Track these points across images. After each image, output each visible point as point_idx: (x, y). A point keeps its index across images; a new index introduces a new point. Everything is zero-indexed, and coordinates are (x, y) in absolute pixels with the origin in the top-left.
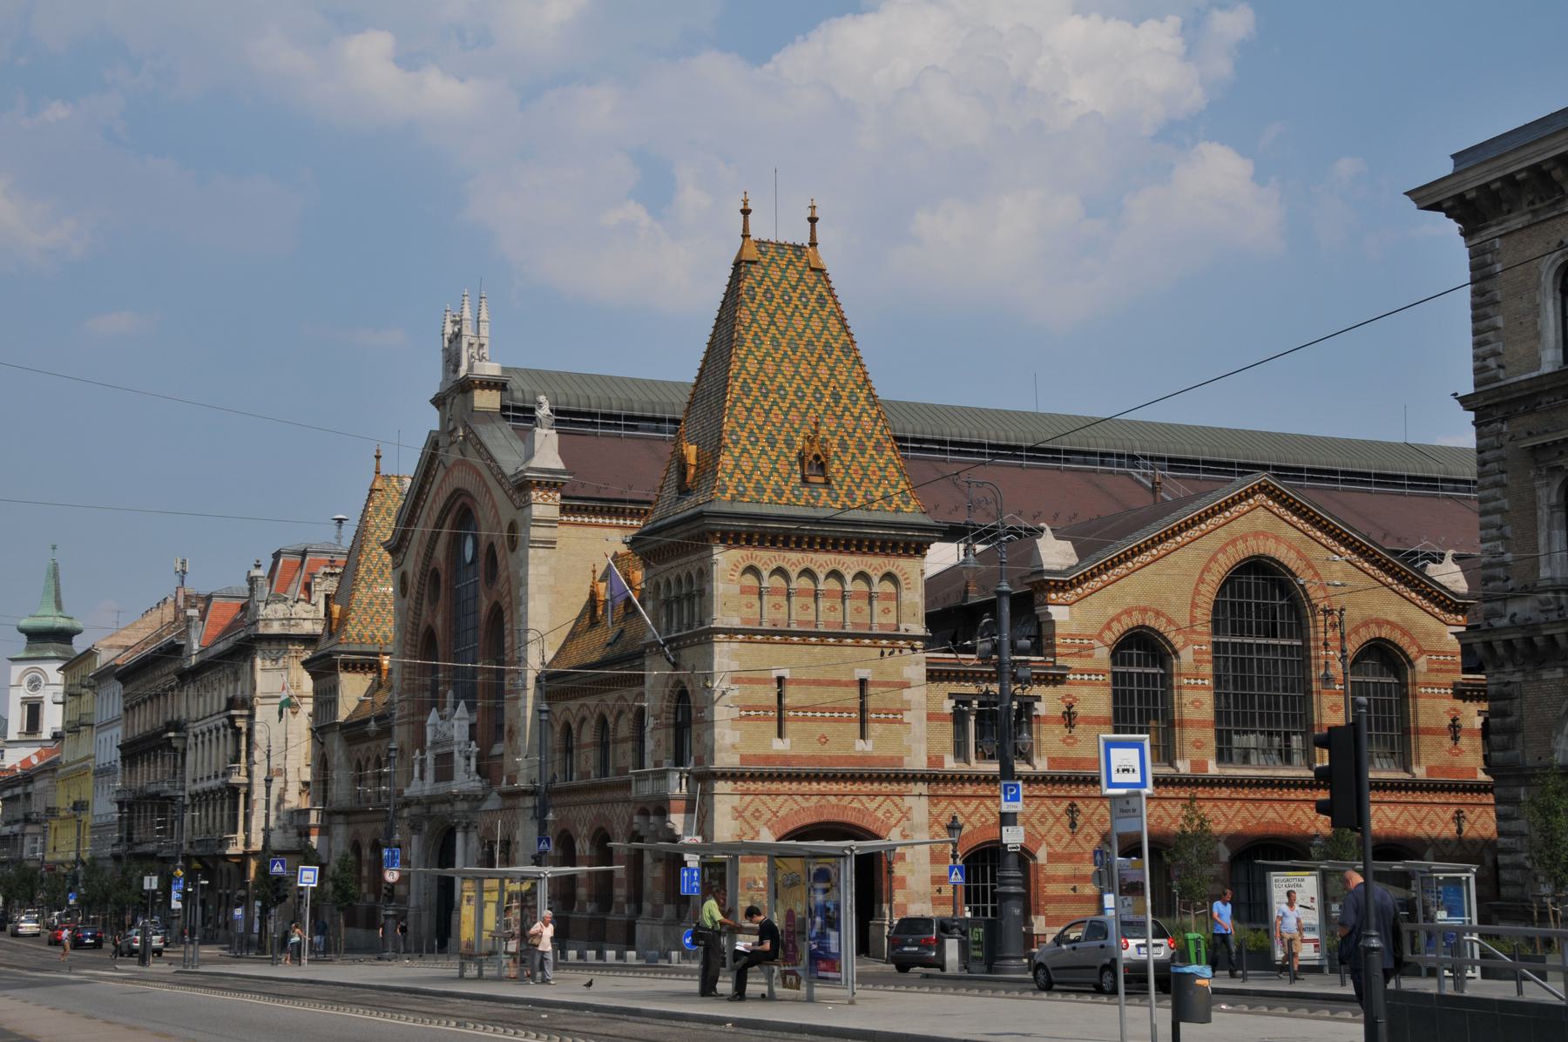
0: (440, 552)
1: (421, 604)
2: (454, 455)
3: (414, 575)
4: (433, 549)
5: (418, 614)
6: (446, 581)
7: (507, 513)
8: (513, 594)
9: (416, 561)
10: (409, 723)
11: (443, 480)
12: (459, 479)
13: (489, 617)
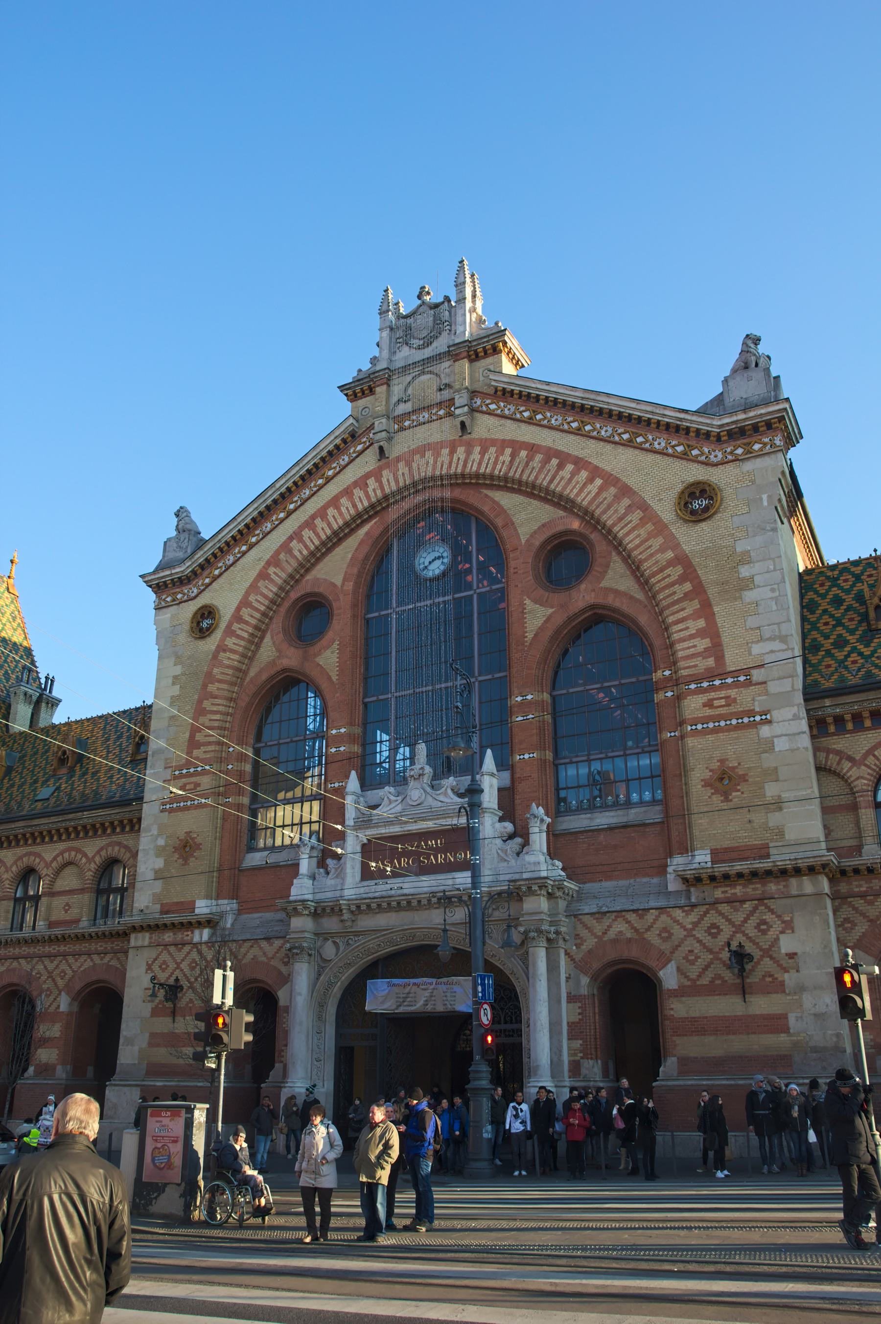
1: (258, 646)
3: (244, 603)
4: (308, 570)
5: (249, 656)
6: (354, 606)
8: (707, 575)
9: (253, 588)
11: (376, 474)
12: (424, 467)
13: (558, 631)
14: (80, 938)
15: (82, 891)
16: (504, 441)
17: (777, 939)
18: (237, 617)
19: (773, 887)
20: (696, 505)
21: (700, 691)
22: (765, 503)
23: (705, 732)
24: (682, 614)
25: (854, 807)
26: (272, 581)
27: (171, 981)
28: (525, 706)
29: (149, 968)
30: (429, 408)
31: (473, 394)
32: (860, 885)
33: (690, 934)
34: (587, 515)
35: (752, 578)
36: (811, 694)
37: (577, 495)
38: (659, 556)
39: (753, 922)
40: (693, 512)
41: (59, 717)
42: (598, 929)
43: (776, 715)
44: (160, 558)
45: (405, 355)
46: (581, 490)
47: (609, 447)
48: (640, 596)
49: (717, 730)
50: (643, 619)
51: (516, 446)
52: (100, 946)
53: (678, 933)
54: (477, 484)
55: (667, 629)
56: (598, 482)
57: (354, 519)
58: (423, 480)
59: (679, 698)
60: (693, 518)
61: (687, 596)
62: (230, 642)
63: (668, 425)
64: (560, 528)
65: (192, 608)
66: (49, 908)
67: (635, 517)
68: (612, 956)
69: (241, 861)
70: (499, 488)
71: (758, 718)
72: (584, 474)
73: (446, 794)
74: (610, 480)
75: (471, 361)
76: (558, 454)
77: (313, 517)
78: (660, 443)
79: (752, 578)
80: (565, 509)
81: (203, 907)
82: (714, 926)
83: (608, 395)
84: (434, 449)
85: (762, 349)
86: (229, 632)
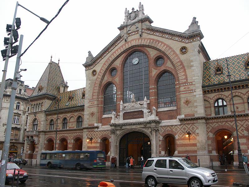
0: (118, 63)
1: (104, 77)
2: (137, 36)
3: (101, 69)
4: (112, 63)
5: (102, 79)
6: (121, 70)
7: (176, 45)
8: (185, 64)
9: (103, 66)
10: (97, 107)
12: (134, 43)
14: (75, 130)
15: (74, 122)
16: (148, 38)
17: (195, 131)
18: (100, 72)
19: (195, 122)
20: (183, 51)
21: (184, 86)
22: (196, 50)
23: (184, 93)
24: (180, 72)
25: (210, 107)
26: (106, 65)
27: (91, 138)
28: (152, 89)
29: (87, 135)
30: (134, 32)
31: (142, 29)
32: (211, 121)
33: (180, 129)
34: (163, 53)
35: (193, 65)
36: (203, 87)
37: (162, 49)
38: (176, 60)
39: (191, 127)
40: (183, 52)
41: (69, 89)
42: (165, 129)
43: (197, 90)
44: (86, 61)
45: (130, 22)
46: (163, 47)
47: (167, 39)
48: (173, 68)
49: (186, 93)
50: (173, 72)
51: (150, 39)
52: (78, 132)
53: (178, 129)
54: (143, 46)
55: (178, 74)
56: (165, 46)
57: (121, 53)
58: (133, 46)
59: (179, 87)
60: (183, 53)
61: (181, 68)
62: (99, 77)
63: (178, 35)
64: (158, 55)
65: (92, 70)
66: (69, 125)
67: (172, 53)
68: (167, 133)
69: (102, 116)
70: (147, 47)
71: (193, 91)
72: (163, 45)
73: (138, 104)
74: (168, 46)
75: (142, 23)
76: (158, 41)
77: (113, 53)
78: (177, 39)
79: (193, 65)
80: (159, 51)
81: (96, 125)
82: (184, 128)
83: (167, 30)
84: (135, 40)
85: (197, 20)
86: (99, 75)
